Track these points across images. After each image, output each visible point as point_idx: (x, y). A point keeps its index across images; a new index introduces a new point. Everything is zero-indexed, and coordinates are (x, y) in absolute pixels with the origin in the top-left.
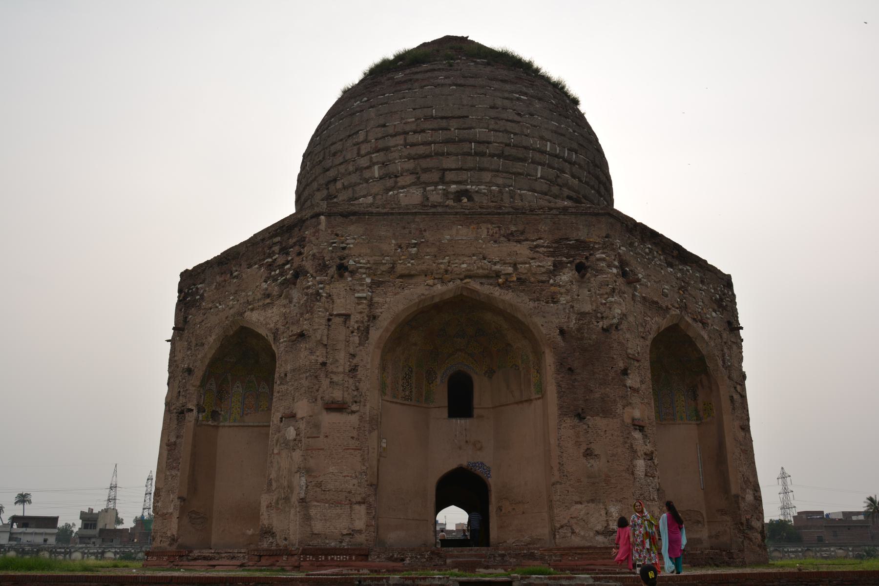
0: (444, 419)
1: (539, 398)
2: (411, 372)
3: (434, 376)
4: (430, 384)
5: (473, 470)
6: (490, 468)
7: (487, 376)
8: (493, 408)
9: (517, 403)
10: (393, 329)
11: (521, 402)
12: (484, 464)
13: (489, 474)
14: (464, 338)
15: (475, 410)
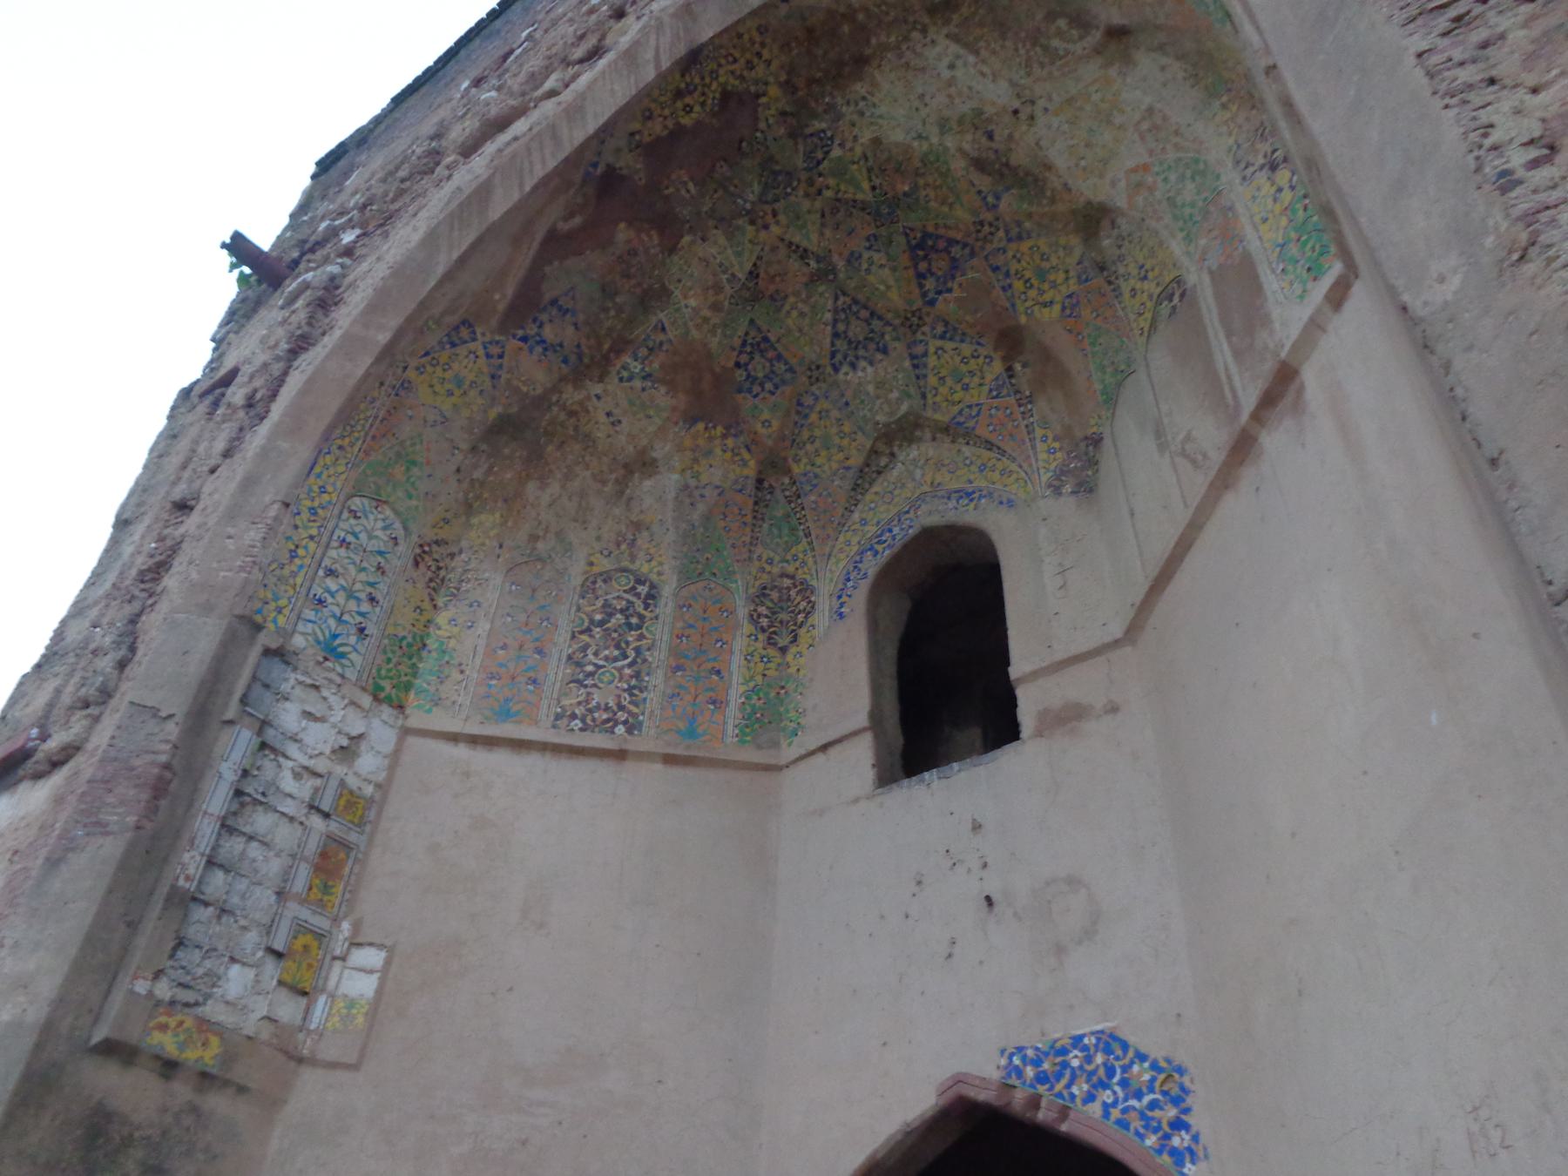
0: (856, 800)
1: (1338, 297)
2: (651, 597)
3: (804, 604)
4: (783, 650)
5: (1042, 1116)
6: (1181, 1070)
7: (1068, 488)
8: (1133, 631)
9: (1224, 481)
10: (383, 338)
11: (1243, 448)
12: (1125, 1046)
13: (1178, 1125)
14: (885, 351)
15: (1020, 693)
